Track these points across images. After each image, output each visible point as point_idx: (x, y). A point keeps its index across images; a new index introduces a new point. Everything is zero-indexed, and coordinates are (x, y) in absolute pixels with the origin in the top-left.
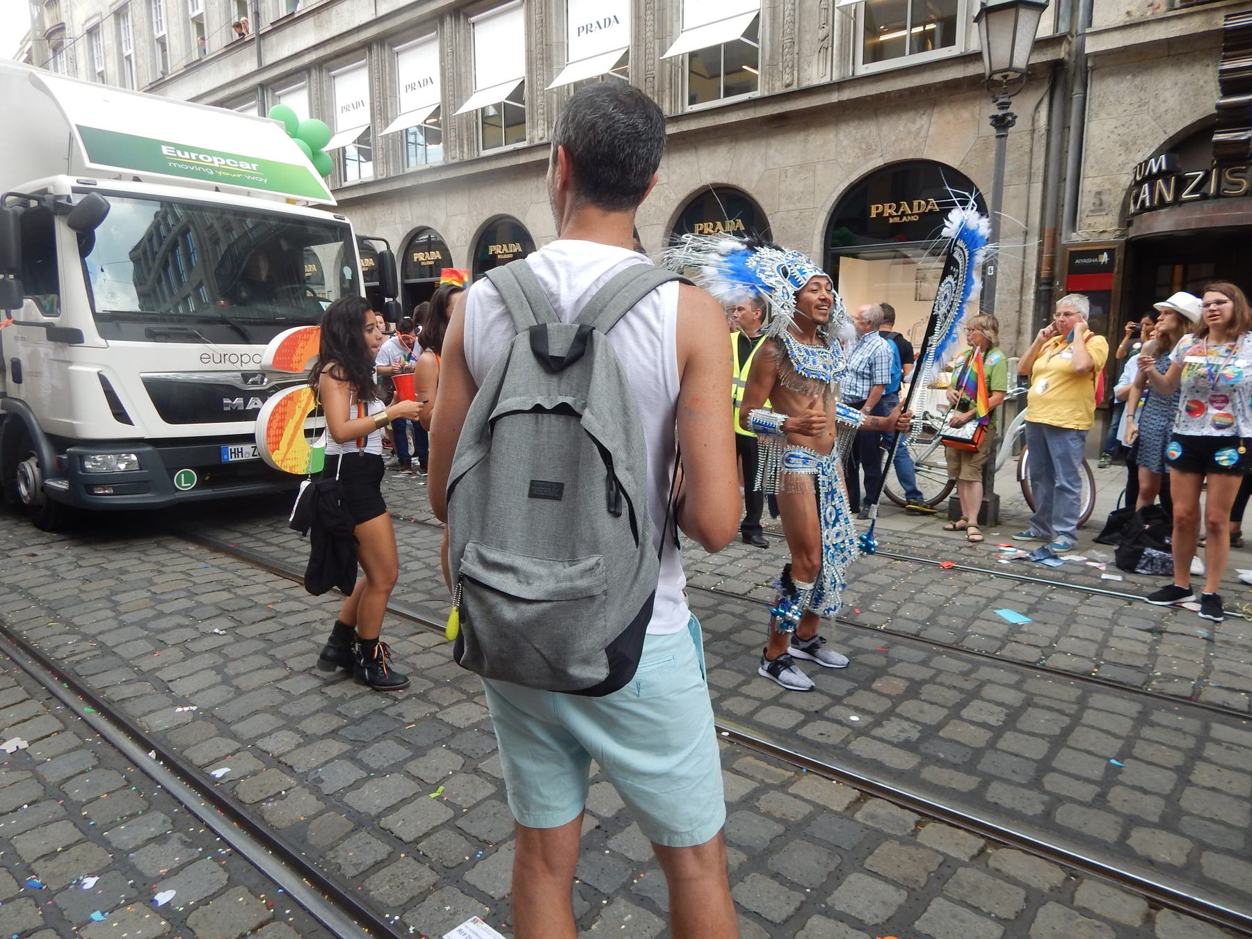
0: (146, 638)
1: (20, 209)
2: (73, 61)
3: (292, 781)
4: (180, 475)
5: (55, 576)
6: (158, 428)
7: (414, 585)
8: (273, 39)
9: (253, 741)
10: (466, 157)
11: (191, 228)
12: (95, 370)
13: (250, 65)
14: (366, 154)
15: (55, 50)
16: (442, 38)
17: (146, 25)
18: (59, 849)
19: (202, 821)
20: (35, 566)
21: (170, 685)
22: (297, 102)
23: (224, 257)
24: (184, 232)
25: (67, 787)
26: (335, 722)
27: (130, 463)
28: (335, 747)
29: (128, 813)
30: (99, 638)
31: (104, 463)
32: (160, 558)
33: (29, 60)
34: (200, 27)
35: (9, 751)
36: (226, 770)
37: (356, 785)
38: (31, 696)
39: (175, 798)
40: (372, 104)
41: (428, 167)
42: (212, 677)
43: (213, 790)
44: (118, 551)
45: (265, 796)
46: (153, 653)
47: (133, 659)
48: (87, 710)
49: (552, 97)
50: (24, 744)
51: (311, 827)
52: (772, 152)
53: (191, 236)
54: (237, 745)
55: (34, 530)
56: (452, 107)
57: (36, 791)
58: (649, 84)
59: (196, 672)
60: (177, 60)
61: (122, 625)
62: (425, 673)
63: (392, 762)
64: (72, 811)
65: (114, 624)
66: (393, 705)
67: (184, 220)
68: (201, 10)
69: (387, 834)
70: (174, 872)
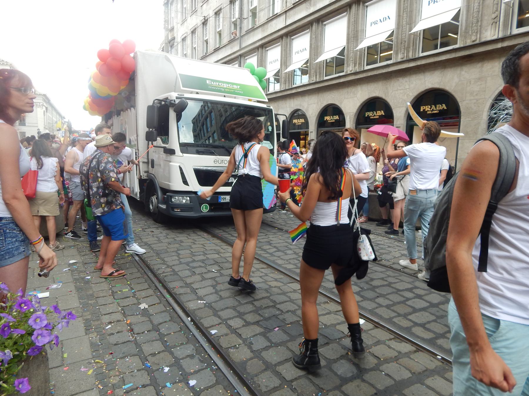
0: (189, 269)
1: (159, 105)
2: (177, 50)
3: (241, 342)
4: (203, 206)
5: (159, 241)
6: (194, 185)
7: (289, 261)
8: (246, 37)
9: (226, 320)
10: (318, 80)
11: (213, 111)
12: (178, 165)
13: (236, 48)
14: (277, 81)
15: (171, 47)
16: (311, 32)
17: (202, 36)
18: (157, 353)
19: (206, 352)
20: (153, 236)
21: (197, 291)
22: (253, 61)
23: (223, 122)
24: (211, 112)
25: (160, 327)
26: (258, 318)
27: (187, 200)
28: (258, 330)
29: (180, 342)
30: (173, 267)
31: (178, 199)
32: (194, 238)
33: (163, 51)
34: (220, 35)
35: (142, 308)
36: (216, 331)
37: (266, 348)
38: (150, 287)
39: (197, 340)
40: (281, 60)
41: (302, 84)
42: (211, 290)
43: (211, 339)
44: (180, 233)
45: (230, 346)
46: (191, 276)
47: (184, 278)
48: (168, 296)
49: (357, 53)
50: (147, 307)
51: (248, 364)
52: (463, 73)
53: (213, 114)
54: (220, 321)
55: (153, 222)
56: (313, 60)
57: (150, 327)
58: (403, 45)
59: (206, 287)
60: (211, 48)
61: (181, 263)
62: (295, 301)
63: (281, 341)
64: (161, 338)
65: (178, 262)
66: (281, 314)
67: (211, 108)
68: (221, 28)
69: (278, 375)
70: (196, 372)
